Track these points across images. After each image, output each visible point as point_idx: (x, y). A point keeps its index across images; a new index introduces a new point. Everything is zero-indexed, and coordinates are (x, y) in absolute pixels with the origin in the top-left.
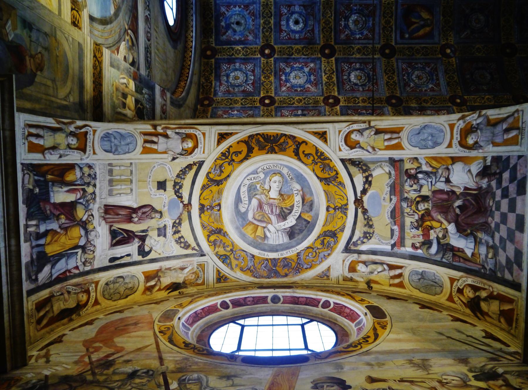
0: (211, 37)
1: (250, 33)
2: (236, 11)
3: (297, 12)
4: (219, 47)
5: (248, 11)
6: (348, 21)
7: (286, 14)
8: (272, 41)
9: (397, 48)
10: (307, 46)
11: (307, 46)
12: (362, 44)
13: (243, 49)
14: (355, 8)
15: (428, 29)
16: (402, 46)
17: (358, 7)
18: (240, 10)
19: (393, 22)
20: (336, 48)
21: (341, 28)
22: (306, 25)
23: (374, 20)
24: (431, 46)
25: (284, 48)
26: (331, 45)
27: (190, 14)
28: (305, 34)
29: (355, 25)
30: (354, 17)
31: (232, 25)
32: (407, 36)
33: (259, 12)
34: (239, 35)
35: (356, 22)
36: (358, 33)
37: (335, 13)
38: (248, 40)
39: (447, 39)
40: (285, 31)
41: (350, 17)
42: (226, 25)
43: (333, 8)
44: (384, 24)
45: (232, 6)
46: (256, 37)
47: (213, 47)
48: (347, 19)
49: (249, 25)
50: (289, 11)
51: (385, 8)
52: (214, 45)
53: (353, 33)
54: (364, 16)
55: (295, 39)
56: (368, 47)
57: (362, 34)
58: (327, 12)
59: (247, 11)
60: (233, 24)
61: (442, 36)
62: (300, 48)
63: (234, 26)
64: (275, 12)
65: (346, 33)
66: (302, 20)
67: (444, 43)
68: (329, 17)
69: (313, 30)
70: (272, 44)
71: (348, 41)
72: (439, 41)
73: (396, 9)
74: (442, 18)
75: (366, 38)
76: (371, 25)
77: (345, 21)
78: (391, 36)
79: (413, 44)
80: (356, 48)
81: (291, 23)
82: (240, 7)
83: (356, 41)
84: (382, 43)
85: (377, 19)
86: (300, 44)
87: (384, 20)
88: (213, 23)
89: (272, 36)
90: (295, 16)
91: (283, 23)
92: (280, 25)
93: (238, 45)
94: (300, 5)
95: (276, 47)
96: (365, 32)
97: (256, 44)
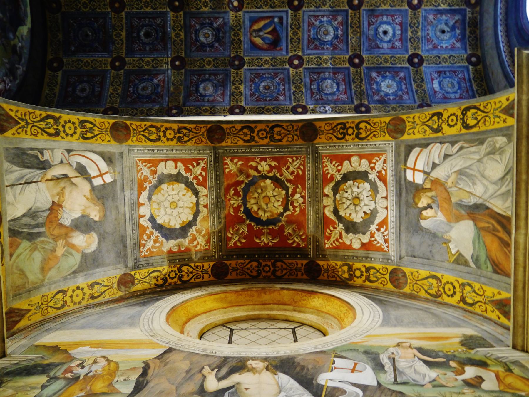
0: (469, 18)
1: (432, 22)
2: (446, 43)
3: (385, 42)
4: (463, 7)
5: (433, 43)
6: (334, 35)
7: (396, 40)
8: (409, 13)
9: (287, 6)
10: (376, 8)
11: (376, 8)
12: (320, 11)
13: (439, 5)
14: (328, 46)
15: (256, 27)
16: (281, 9)
17: (325, 47)
18: (441, 45)
19: (290, 34)
20: (347, 6)
21: (342, 28)
22: (376, 30)
23: (309, 36)
24: (252, 10)
25: (399, 5)
26: (352, 9)
27: (503, 15)
28: (377, 21)
29: (327, 30)
30: (329, 38)
31: (449, 30)
32: (276, 20)
33: (422, 43)
35: (327, 33)
36: (325, 23)
37: (347, 42)
38: (434, 15)
39: (236, 17)
40: (396, 24)
41: (333, 38)
42: (455, 30)
43: (350, 46)
44: (299, 31)
45: (449, 47)
46: (426, 18)
47: (469, 8)
48: (336, 37)
49: (432, 30)
50: (393, 44)
51: (298, 47)
52: (468, 9)
53: (330, 22)
54: (319, 39)
55: (387, 15)
56: (316, 7)
57: (321, 22)
58: (355, 42)
59: (435, 44)
60: (448, 31)
61: (241, 21)
62: (383, 5)
63: (446, 29)
64: (407, 42)
65: (336, 22)
66: (380, 35)
67: (240, 13)
68: (353, 38)
69: (369, 25)
70: (410, 10)
71: (334, 13)
72: (244, 15)
73: (287, 46)
74: (242, 39)
75: (316, 17)
76: (312, 31)
77: (337, 35)
78: (292, 20)
79: (270, 12)
80: (327, 6)
81: (391, 32)
82: (442, 47)
83: (327, 13)
84: (301, 12)
85: (306, 37)
86: (382, 10)
87: (299, 35)
88: (467, 32)
89: (409, 18)
90: (386, 38)
91: (398, 32)
92: (401, 30)
93: (444, 9)
94: (383, 48)
95: (407, 7)
96: (317, 23)
97: (425, 10)
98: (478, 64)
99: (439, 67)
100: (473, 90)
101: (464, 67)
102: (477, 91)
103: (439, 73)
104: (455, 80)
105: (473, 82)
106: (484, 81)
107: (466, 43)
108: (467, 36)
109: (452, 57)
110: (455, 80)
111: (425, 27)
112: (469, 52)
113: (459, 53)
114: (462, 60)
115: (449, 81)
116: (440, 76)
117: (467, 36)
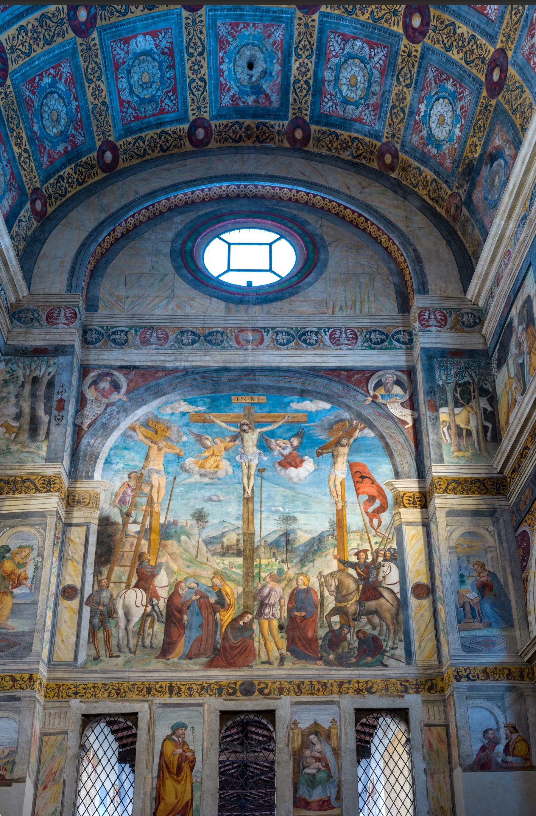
1: (269, 36)
2: (229, 70)
13: (299, 56)
34: (271, 62)
42: (253, 93)
60: (251, 76)
63: (256, 72)
88: (249, 122)
97: (292, 20)
98: (191, 142)
99: (181, 52)
100: (141, 130)
101: (186, 111)
102: (140, 138)
103: (170, 53)
104: (158, 90)
105: (159, 131)
106: (161, 154)
107: (230, 118)
108: (241, 121)
109: (203, 84)
110: (158, 90)
111: (261, 20)
112: (213, 123)
113: (211, 100)
114: (199, 108)
115: (154, 75)
116: (164, 53)
117: (241, 121)
